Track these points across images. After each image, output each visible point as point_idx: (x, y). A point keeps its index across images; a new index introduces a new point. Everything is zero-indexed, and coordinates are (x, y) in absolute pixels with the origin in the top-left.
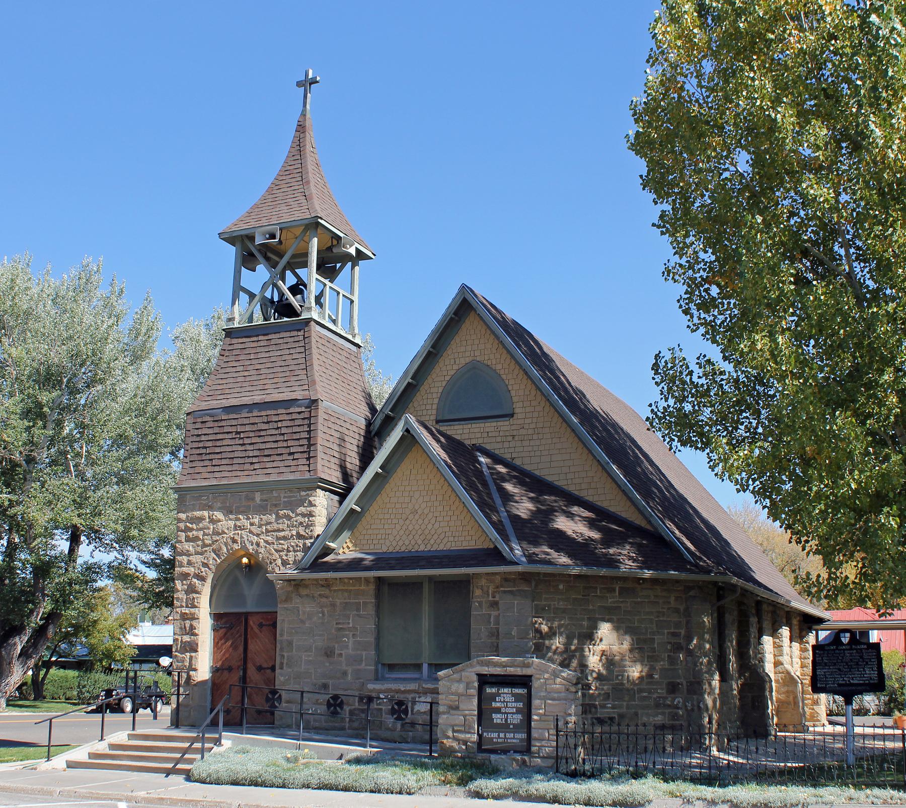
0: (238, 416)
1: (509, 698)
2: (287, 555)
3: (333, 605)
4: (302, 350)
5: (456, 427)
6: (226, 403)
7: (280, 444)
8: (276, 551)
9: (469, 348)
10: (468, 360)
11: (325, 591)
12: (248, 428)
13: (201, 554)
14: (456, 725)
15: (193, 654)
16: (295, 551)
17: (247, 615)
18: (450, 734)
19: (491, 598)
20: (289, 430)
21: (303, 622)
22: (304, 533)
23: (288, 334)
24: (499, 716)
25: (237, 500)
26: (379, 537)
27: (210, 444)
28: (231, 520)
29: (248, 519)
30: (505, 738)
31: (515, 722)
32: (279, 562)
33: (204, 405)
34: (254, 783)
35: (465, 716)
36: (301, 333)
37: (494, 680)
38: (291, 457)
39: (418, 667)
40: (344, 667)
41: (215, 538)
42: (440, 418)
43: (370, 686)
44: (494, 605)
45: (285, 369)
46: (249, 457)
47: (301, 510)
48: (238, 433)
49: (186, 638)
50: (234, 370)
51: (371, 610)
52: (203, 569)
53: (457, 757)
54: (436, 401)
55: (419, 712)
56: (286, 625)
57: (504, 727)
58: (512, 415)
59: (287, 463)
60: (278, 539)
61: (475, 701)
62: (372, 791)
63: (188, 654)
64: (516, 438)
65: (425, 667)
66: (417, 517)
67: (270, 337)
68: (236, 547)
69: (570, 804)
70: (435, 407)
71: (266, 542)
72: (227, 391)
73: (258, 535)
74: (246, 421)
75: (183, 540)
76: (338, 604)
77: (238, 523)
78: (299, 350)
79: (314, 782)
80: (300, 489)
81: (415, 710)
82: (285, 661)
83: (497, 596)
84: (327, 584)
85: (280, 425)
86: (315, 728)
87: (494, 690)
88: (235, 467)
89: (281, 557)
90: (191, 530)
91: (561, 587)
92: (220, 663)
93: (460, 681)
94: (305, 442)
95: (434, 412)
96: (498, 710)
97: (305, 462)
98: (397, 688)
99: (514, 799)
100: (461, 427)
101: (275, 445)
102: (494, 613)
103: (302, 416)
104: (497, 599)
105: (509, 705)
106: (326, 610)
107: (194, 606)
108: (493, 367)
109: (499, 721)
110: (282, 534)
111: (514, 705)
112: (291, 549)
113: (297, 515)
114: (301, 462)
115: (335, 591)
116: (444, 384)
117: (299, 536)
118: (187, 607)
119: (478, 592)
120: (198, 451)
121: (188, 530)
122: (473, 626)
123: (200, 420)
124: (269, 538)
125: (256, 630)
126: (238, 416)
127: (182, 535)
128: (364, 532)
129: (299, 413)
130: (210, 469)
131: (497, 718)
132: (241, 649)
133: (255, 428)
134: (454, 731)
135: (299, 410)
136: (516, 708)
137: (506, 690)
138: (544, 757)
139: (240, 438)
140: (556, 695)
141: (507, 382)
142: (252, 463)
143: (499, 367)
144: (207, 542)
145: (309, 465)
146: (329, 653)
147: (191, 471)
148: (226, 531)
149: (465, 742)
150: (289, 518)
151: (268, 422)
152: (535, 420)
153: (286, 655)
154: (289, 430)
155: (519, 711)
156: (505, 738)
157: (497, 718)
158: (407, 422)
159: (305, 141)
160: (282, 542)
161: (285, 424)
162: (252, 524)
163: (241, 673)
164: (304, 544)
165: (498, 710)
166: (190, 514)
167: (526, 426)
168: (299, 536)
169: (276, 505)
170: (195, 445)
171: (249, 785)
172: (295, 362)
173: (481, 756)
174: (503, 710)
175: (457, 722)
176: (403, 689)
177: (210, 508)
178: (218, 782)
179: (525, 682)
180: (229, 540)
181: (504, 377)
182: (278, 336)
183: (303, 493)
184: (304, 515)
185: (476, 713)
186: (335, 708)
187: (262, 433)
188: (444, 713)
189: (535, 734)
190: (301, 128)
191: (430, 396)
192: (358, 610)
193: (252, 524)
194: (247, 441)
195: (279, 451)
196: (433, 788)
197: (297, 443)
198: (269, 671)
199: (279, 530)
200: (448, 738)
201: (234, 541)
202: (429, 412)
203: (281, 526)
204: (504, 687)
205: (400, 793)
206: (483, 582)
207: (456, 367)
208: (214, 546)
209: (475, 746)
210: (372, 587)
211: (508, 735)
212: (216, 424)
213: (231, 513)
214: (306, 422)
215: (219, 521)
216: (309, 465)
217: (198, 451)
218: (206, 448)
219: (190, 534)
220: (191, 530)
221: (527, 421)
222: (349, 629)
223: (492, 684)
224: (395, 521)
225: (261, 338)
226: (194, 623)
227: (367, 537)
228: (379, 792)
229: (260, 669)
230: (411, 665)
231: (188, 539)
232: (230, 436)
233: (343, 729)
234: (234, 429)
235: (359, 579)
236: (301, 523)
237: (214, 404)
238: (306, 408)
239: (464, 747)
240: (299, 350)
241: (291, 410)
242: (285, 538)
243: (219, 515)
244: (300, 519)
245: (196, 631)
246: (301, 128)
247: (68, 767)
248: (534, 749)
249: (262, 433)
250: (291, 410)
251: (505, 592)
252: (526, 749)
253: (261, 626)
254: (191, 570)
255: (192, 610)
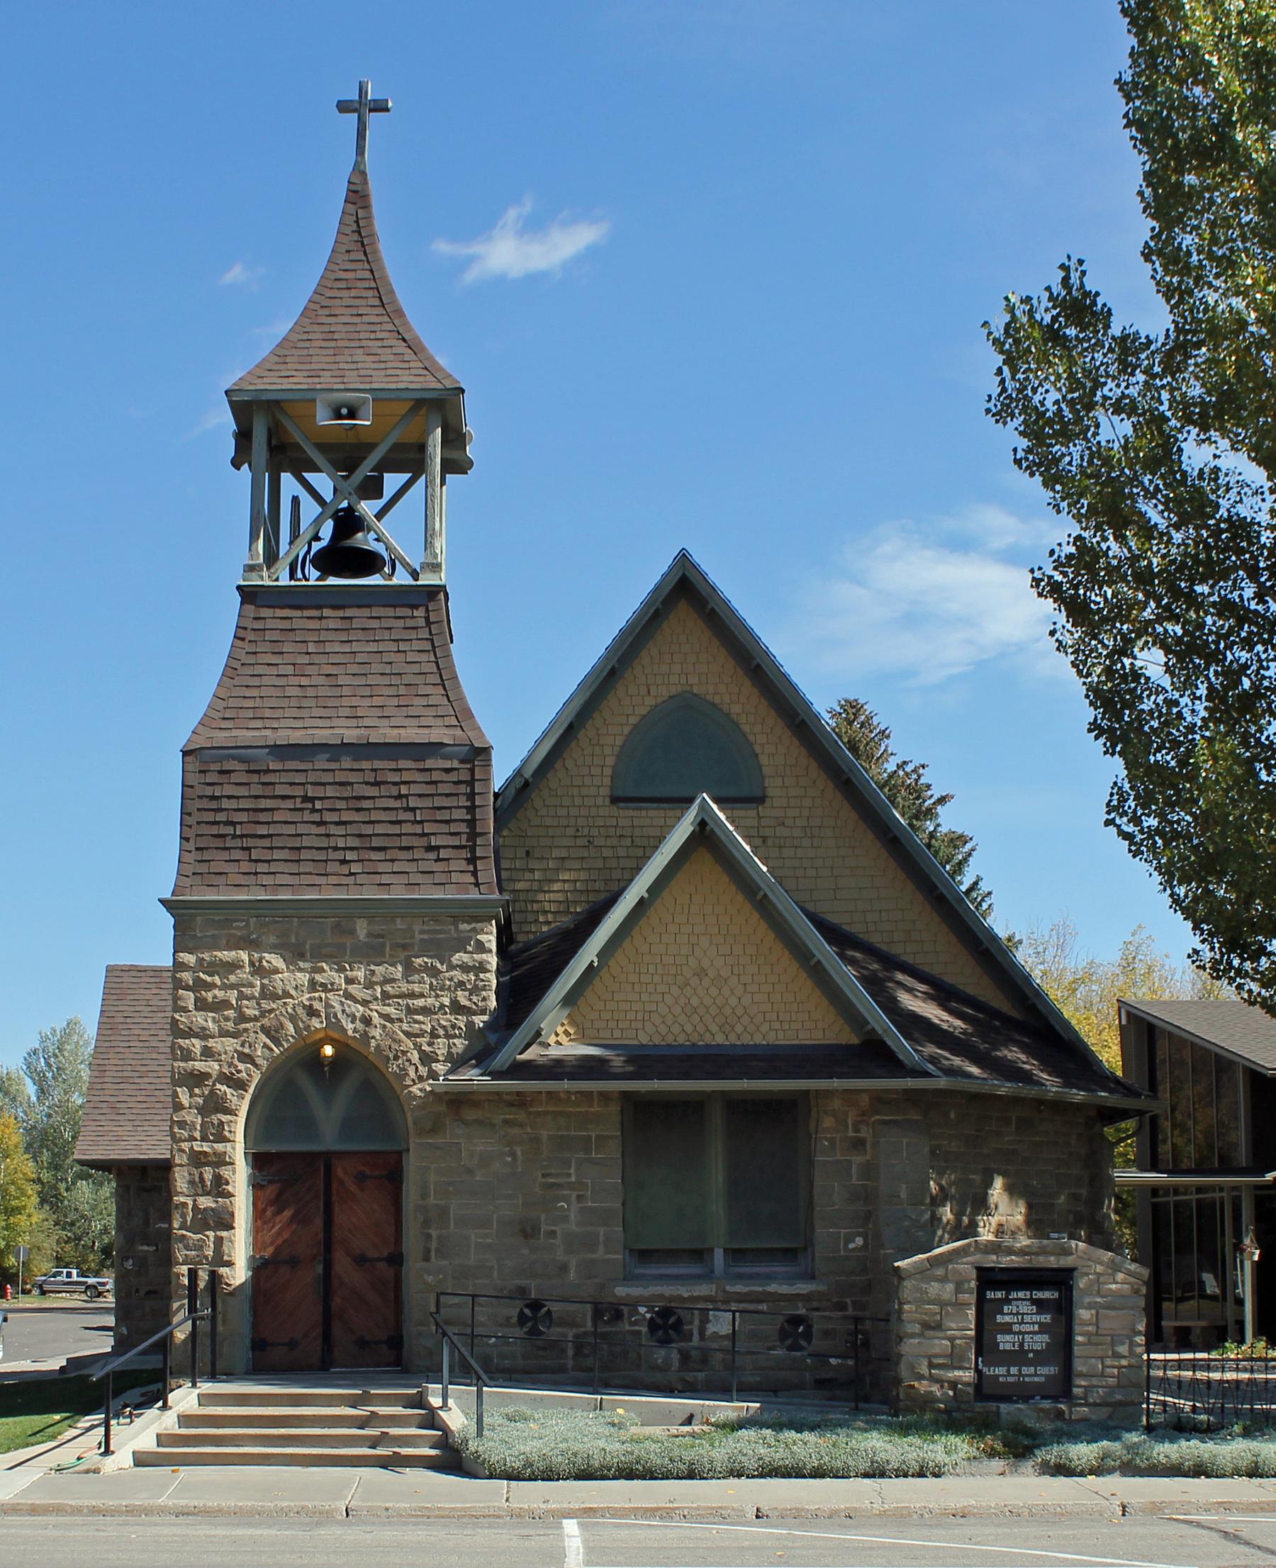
0: (309, 766)
1: (1026, 1308)
2: (430, 1044)
3: (536, 1140)
4: (428, 646)
5: (652, 813)
6: (271, 737)
7: (406, 828)
8: (407, 1034)
9: (677, 668)
10: (674, 691)
11: (521, 1116)
12: (330, 791)
13: (234, 1035)
14: (937, 1356)
15: (224, 1234)
16: (448, 1036)
17: (328, 1158)
18: (924, 1370)
19: (851, 1134)
20: (427, 803)
21: (470, 1171)
22: (467, 1003)
23: (390, 612)
24: (1008, 1338)
25: (314, 934)
26: (631, 1016)
27: (242, 817)
28: (301, 970)
29: (341, 970)
30: (1020, 1375)
31: (1038, 1347)
32: (415, 1056)
33: (221, 738)
34: (628, 1473)
35: (952, 1339)
36: (420, 613)
37: (1005, 1278)
38: (433, 855)
39: (700, 1255)
40: (560, 1256)
41: (266, 1005)
42: (620, 793)
43: (621, 1291)
44: (858, 1144)
45: (395, 680)
46: (336, 849)
47: (459, 958)
48: (306, 799)
49: (205, 1202)
50: (274, 671)
51: (613, 1151)
52: (241, 1066)
53: (939, 1410)
54: (610, 761)
55: (716, 1336)
56: (432, 1178)
57: (1018, 1357)
58: (760, 800)
59: (423, 866)
60: (410, 1011)
61: (971, 1313)
62: (866, 1475)
63: (211, 1234)
64: (770, 842)
65: (719, 1255)
66: (706, 982)
67: (349, 613)
68: (316, 1023)
69: (1223, 1476)
70: (608, 772)
71: (387, 1017)
72: (268, 713)
73: (365, 1003)
74: (328, 778)
75: (191, 1007)
76: (545, 1138)
77: (318, 978)
78: (417, 645)
79: (751, 1464)
80: (456, 919)
81: (708, 1333)
82: (434, 1245)
83: (864, 1128)
84: (521, 1101)
85: (404, 790)
86: (502, 1371)
87: (999, 1295)
88: (305, 867)
89: (418, 1047)
90: (213, 986)
91: (952, 1115)
92: (271, 1249)
93: (943, 1280)
94: (463, 828)
95: (607, 781)
96: (1007, 1329)
97: (463, 865)
98: (675, 1293)
99: (1124, 1475)
100: (662, 813)
101: (395, 829)
102: (858, 1159)
103: (453, 777)
104: (862, 1135)
105: (1027, 1319)
106: (518, 1150)
107: (221, 1139)
108: (725, 708)
109: (1008, 1347)
110: (420, 1002)
111: (1036, 1318)
112: (442, 1032)
113: (452, 967)
114: (454, 866)
115: (538, 1114)
116: (626, 730)
117: (457, 1008)
118: (204, 1139)
119: (828, 1122)
120: (214, 830)
121: (199, 985)
122: (818, 1181)
123: (217, 767)
124: (390, 1010)
125: (353, 1188)
126: (309, 766)
127: (189, 998)
128: (600, 1005)
129: (448, 771)
130: (246, 867)
131: (1006, 1342)
132: (319, 1222)
133: (347, 792)
134: (931, 1366)
135: (448, 765)
136: (1040, 1324)
137: (1021, 1294)
138: (1095, 1405)
139: (314, 810)
140: (764, 1307)
141: (751, 738)
142: (344, 862)
143: (736, 709)
144: (250, 1012)
145: (475, 873)
146: (528, 1231)
147: (203, 868)
148: (293, 992)
149: (953, 1384)
150: (434, 972)
151: (377, 784)
152: (806, 813)
153: (434, 1233)
154: (427, 803)
155: (1043, 1328)
156: (1020, 1375)
157: (1006, 1342)
158: (704, 806)
159: (371, 225)
160: (420, 1018)
161: (415, 789)
162: (350, 981)
163: (320, 1269)
164: (470, 1025)
165: (1007, 1329)
166: (206, 956)
167: (788, 822)
168: (457, 1008)
169: (404, 947)
170: (210, 817)
171: (615, 1478)
172: (415, 669)
173: (979, 1407)
174: (1016, 1328)
175: (937, 1350)
176: (686, 1295)
177: (251, 944)
178: (549, 1475)
179: (1062, 1279)
180: (300, 1011)
181: (746, 728)
182: (366, 612)
183: (464, 927)
184: (465, 968)
185: (972, 1333)
186: (666, 1333)
187: (366, 804)
188: (913, 1336)
189: (1079, 1366)
190: (358, 197)
191: (598, 751)
192: (587, 1150)
193: (350, 981)
194: (329, 817)
195: (405, 842)
196: (975, 1463)
197: (444, 828)
198: (382, 1265)
199: (412, 995)
200: (920, 1377)
201: (312, 1012)
202: (597, 781)
203: (416, 988)
204: (1018, 1290)
205: (921, 1474)
206: (836, 1104)
207: (650, 701)
208: (265, 1021)
209: (971, 1390)
210: (615, 1108)
211: (1025, 1370)
212: (255, 778)
213: (302, 956)
214: (463, 789)
215: (276, 971)
216: (475, 873)
217: (214, 830)
218: (233, 824)
219: (209, 996)
220: (213, 986)
221: (790, 813)
222: (570, 1186)
223: (996, 1285)
224: (660, 988)
225: (326, 612)
226: (225, 1172)
227: (605, 1016)
228: (882, 1475)
229: (361, 1260)
230: (684, 1251)
231: (201, 1005)
232: (289, 804)
233: (562, 1369)
234: (298, 791)
235: (587, 1095)
236: (461, 984)
237: (245, 737)
238: (462, 762)
239: (951, 1393)
240: (417, 645)
241: (429, 763)
242: (425, 1011)
243: (277, 961)
244: (458, 975)
245: (230, 1188)
246: (358, 197)
247: (136, 1465)
248: (1076, 1391)
249: (366, 804)
250: (429, 763)
251: (885, 1123)
252: (1063, 1387)
253: (361, 1178)
254: (213, 1067)
255: (219, 1147)
